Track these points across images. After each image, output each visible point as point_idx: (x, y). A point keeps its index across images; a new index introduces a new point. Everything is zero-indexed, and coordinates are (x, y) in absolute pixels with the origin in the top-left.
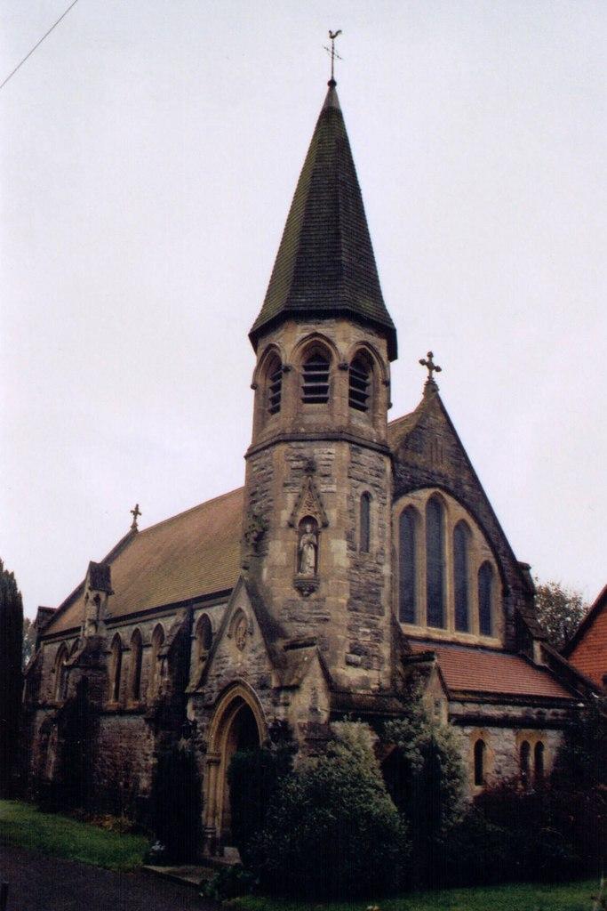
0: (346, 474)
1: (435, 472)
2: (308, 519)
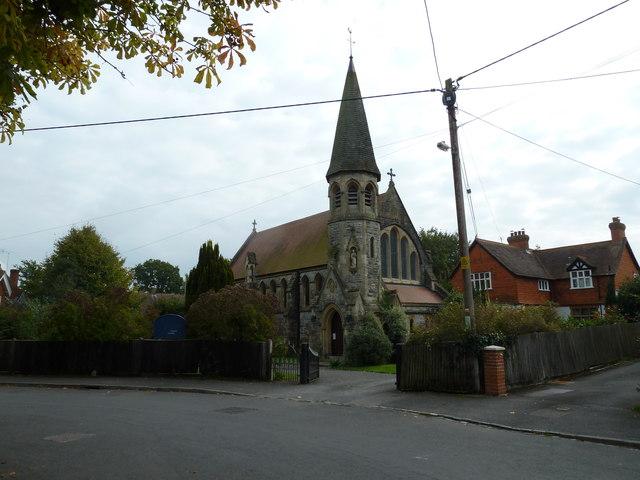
2: (353, 248)
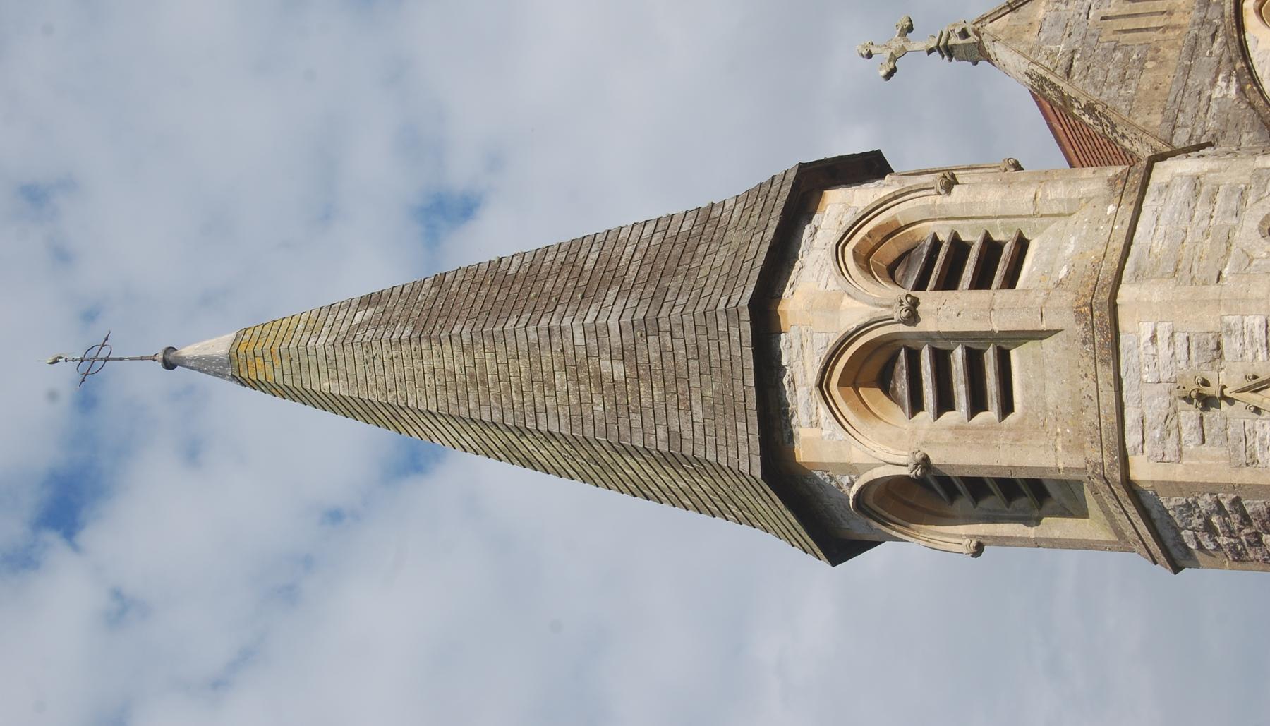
0: (1213, 289)
1: (1196, 15)
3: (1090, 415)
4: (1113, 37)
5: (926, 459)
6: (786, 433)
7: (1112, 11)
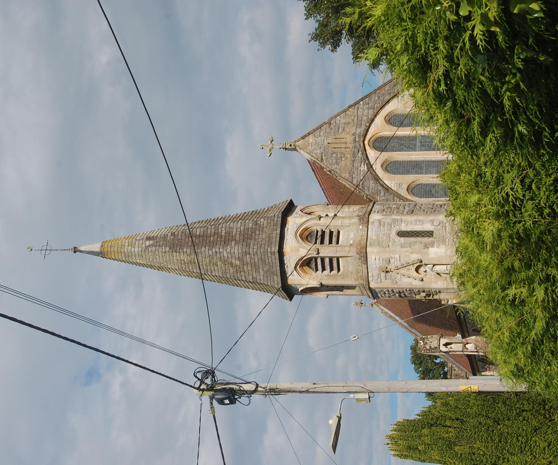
0: (388, 249)
3: (361, 274)
4: (332, 149)
5: (321, 283)
6: (285, 278)
7: (330, 141)
